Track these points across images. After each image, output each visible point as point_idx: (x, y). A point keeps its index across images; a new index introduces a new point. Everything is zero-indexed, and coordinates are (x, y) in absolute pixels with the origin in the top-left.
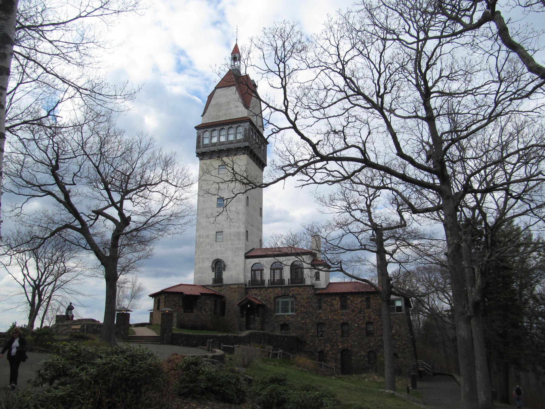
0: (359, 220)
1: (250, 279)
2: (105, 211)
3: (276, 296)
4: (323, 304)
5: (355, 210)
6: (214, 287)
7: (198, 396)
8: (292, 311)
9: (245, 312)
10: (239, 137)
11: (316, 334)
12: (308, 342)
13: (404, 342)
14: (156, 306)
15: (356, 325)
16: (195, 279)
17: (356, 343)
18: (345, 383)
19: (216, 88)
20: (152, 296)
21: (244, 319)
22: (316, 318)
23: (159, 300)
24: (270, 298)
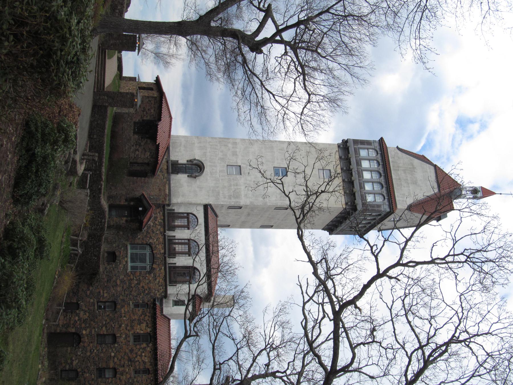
0: (254, 361)
1: (176, 211)
2: (270, 21)
3: (153, 246)
4: (141, 310)
5: (269, 357)
6: (167, 162)
7: (24, 144)
8: (132, 268)
9: (132, 203)
10: (370, 198)
12: (91, 288)
14: (144, 85)
15: (113, 354)
16: (178, 137)
18: (35, 338)
19: (435, 166)
20: (158, 80)
21: (123, 202)
22: (123, 300)
23: (152, 89)
24: (151, 238)
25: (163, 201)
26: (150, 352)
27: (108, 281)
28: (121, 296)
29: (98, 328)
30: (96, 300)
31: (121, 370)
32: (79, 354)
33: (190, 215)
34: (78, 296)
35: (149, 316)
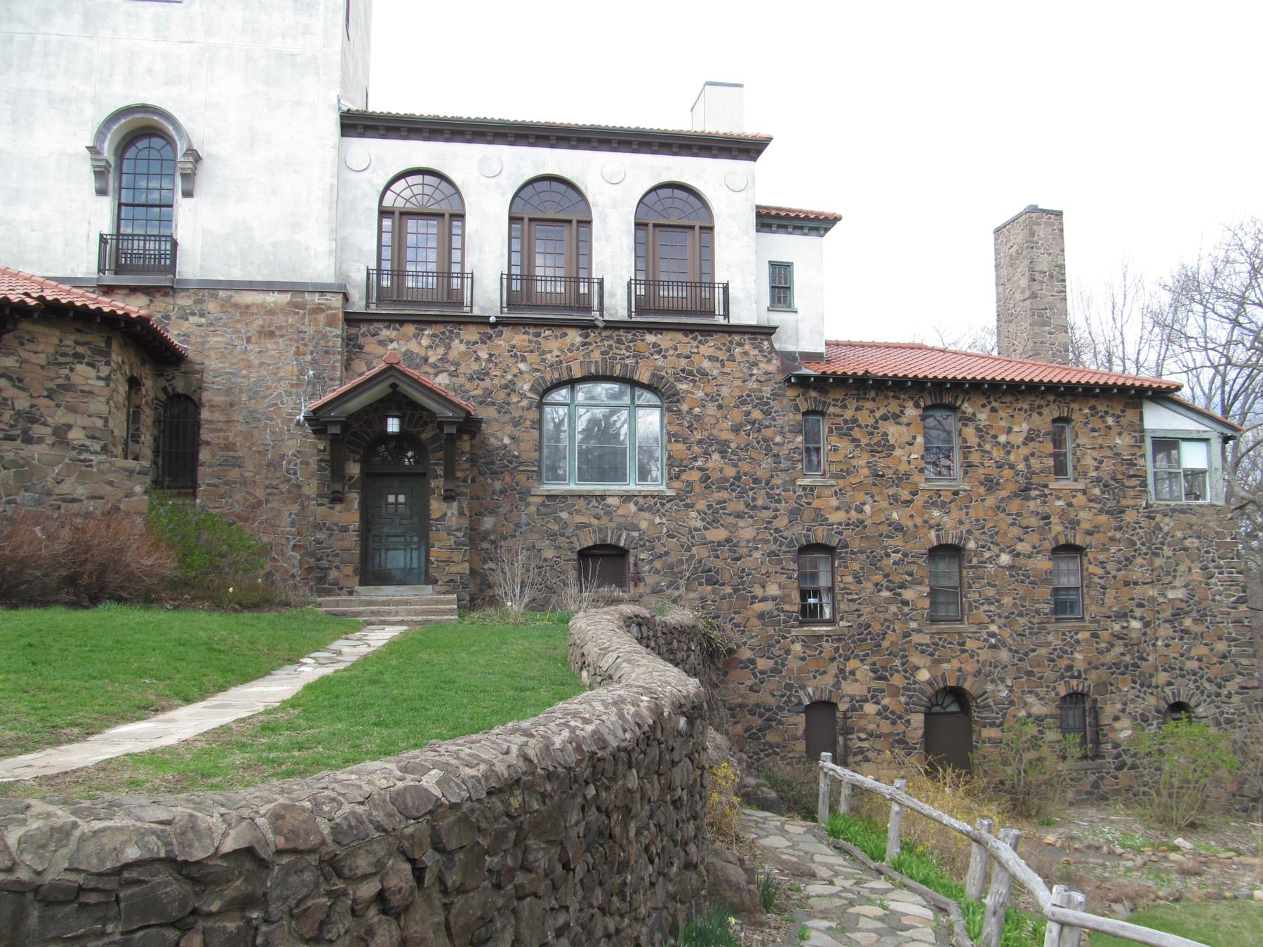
1: (373, 265)
3: (551, 376)
4: (834, 440)
6: (108, 290)
9: (354, 469)
11: (794, 606)
12: (746, 654)
13: (1221, 647)
15: (1005, 559)
17: (1004, 655)
22: (794, 514)
24: (510, 387)
25: (331, 322)
26: (994, 410)
27: (711, 582)
28: (776, 524)
29: (907, 618)
30: (794, 632)
31: (1060, 528)
32: (1005, 693)
33: (385, 204)
34: (780, 709)
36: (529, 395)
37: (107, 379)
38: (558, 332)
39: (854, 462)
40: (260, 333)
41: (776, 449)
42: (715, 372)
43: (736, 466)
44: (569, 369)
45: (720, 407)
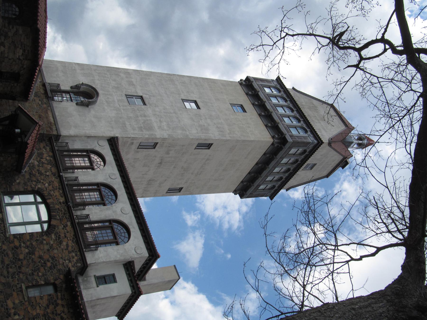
3: (46, 193)
24: (38, 181)
35: (63, 306)
36: (37, 187)
37: (19, 59)
38: (62, 195)
39: (38, 308)
40: (40, 115)
41: (36, 274)
42: (62, 247)
43: (24, 258)
44: (50, 199)
45: (48, 250)
